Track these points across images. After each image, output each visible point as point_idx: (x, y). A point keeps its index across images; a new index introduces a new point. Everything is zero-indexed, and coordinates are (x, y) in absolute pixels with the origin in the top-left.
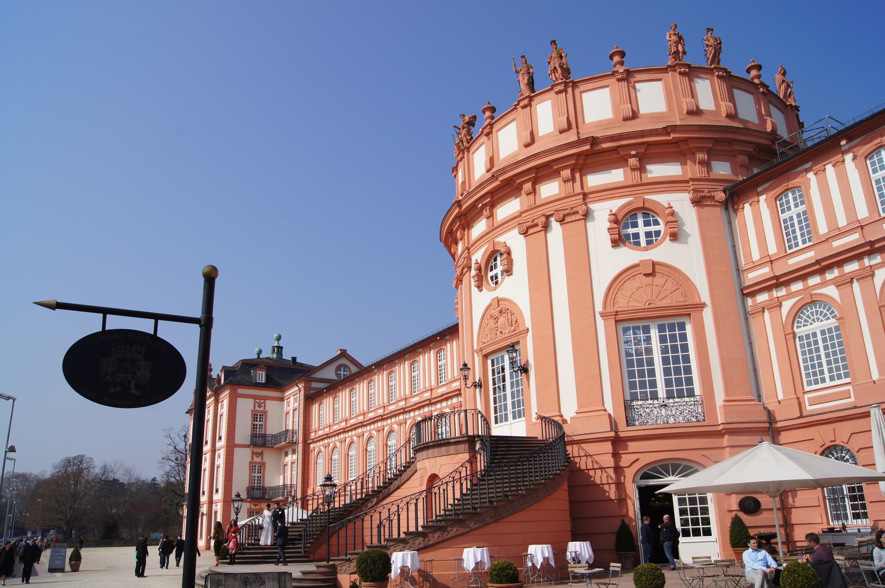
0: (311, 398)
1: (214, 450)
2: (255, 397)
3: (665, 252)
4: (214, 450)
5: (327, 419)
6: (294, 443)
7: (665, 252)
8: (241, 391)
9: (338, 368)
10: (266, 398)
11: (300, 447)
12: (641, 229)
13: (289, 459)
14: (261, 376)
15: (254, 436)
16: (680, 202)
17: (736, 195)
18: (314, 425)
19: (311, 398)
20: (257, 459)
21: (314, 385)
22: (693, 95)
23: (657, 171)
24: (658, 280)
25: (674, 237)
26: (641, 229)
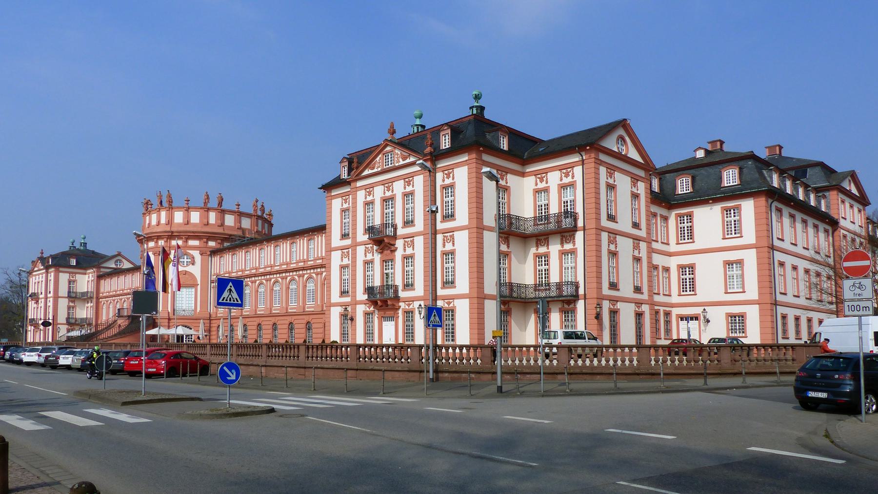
0: (100, 277)
1: (46, 298)
2: (70, 273)
3: (190, 269)
4: (46, 298)
5: (107, 289)
6: (91, 298)
7: (190, 269)
8: (61, 269)
9: (116, 261)
10: (76, 273)
11: (94, 300)
12: (185, 260)
13: (89, 305)
14: (73, 262)
15: (69, 292)
16: (196, 254)
17: (214, 252)
18: (102, 290)
19: (100, 277)
20: (71, 304)
21: (102, 270)
22: (208, 218)
23: (192, 243)
24: (187, 276)
25: (193, 264)
26: (185, 260)
